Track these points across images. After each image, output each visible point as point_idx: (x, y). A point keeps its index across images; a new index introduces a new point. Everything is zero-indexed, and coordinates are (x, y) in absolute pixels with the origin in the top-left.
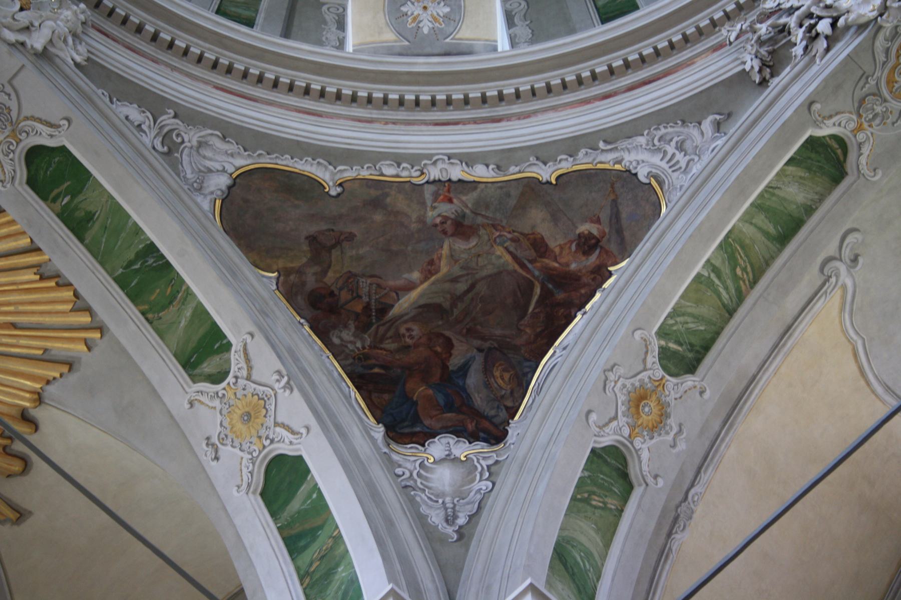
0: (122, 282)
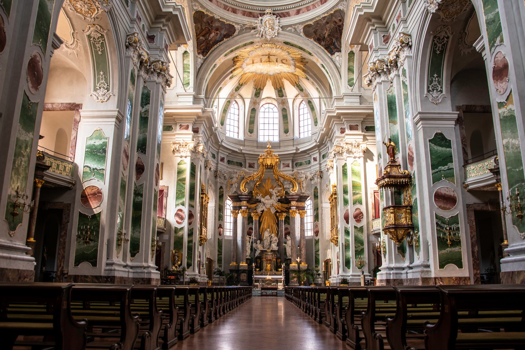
0: (300, 49)
